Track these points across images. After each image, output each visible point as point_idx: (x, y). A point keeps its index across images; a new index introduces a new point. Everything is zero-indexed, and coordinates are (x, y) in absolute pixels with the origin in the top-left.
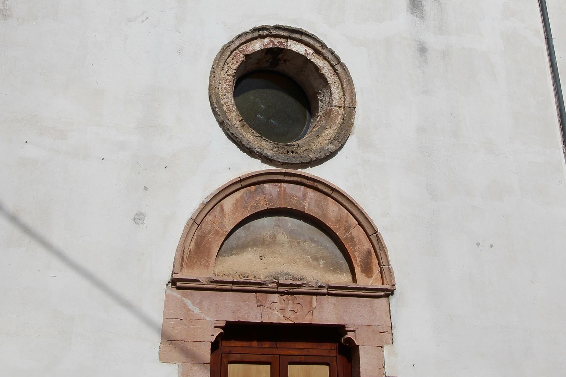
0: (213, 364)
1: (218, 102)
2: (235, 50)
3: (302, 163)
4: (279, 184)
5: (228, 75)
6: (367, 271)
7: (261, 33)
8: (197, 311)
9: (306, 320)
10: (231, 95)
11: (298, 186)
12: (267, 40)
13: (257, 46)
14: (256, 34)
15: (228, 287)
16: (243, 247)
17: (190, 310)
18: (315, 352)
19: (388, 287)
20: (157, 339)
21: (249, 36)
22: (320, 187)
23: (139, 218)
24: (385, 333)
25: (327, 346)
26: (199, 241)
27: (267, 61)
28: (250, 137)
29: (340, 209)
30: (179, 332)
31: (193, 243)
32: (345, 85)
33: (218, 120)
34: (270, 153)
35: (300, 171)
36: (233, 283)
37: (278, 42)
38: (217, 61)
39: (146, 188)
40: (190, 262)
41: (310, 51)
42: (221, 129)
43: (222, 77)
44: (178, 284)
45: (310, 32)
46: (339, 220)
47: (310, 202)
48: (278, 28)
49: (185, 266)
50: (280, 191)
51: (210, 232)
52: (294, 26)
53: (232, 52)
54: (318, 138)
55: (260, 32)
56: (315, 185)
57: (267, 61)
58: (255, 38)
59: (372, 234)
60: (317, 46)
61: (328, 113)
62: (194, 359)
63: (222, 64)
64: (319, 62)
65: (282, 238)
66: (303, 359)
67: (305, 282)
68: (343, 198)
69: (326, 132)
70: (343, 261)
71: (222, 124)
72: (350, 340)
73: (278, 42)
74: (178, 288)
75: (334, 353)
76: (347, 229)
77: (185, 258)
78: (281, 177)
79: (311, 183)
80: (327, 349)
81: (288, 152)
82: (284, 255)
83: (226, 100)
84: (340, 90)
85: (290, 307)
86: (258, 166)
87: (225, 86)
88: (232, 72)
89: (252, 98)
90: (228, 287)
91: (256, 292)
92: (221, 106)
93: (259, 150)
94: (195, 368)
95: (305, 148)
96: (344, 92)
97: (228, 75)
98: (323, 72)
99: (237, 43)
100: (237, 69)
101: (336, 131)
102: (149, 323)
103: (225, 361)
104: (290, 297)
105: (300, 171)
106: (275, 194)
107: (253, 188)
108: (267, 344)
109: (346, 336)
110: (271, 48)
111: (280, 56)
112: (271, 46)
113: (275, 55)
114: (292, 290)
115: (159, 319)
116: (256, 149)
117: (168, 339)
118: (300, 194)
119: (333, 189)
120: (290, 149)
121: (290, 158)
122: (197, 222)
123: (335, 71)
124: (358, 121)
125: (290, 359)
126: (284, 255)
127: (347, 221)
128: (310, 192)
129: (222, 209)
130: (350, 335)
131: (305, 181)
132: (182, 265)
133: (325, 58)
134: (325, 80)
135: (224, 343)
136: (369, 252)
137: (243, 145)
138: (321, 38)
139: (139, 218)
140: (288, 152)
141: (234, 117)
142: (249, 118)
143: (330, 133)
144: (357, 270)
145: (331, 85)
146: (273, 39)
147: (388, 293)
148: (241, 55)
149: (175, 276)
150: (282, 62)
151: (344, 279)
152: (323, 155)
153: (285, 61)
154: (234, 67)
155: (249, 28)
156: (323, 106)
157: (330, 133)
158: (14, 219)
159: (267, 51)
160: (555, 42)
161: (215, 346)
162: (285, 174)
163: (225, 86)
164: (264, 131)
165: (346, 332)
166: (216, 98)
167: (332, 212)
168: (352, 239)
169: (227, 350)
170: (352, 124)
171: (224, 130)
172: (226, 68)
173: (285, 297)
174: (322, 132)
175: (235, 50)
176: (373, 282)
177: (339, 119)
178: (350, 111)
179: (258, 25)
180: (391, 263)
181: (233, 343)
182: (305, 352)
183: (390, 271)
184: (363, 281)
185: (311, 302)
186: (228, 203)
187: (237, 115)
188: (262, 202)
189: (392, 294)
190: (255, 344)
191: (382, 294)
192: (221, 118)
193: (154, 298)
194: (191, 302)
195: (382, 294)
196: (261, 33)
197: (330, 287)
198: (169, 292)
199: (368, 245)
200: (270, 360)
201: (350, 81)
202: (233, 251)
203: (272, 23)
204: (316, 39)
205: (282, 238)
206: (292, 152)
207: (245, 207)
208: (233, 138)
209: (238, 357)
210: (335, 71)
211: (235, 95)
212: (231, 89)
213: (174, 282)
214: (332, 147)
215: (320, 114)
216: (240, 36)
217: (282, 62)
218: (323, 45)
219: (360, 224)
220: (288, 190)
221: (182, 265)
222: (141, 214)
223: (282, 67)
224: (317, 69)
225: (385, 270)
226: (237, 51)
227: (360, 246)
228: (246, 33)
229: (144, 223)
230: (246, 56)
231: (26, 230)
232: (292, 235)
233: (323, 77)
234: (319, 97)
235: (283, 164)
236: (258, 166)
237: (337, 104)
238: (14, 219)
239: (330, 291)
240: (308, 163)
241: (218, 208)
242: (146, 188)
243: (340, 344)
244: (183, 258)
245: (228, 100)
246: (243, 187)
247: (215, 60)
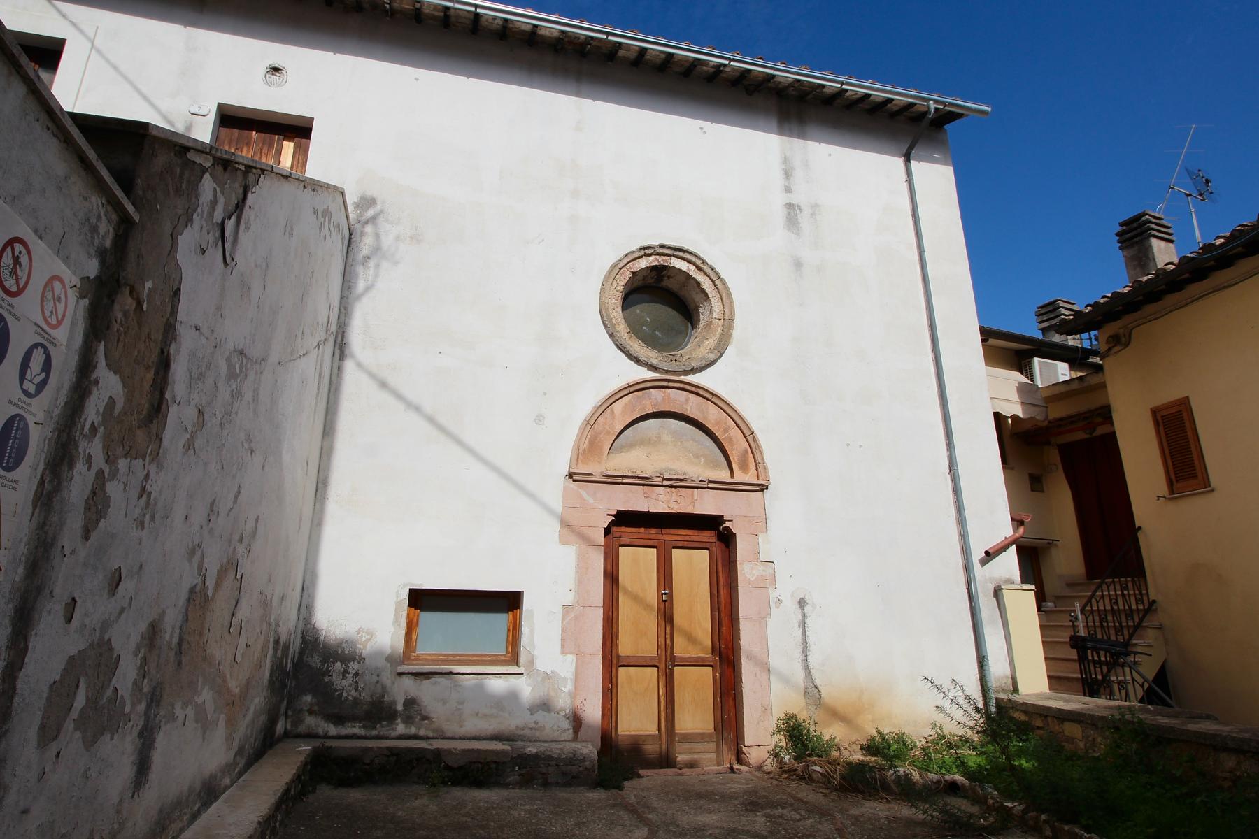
0: (606, 546)
1: (608, 316)
6: (744, 467)
8: (591, 501)
10: (619, 309)
12: (652, 258)
13: (644, 263)
14: (642, 253)
16: (631, 446)
18: (693, 538)
20: (557, 526)
21: (636, 255)
22: (701, 392)
23: (539, 419)
25: (707, 533)
28: (637, 347)
34: (655, 362)
35: (683, 378)
38: (607, 277)
39: (545, 393)
41: (693, 268)
45: (692, 250)
47: (692, 406)
48: (662, 246)
52: (677, 245)
54: (697, 347)
55: (646, 251)
56: (696, 390)
60: (699, 262)
64: (700, 277)
65: (666, 438)
66: (685, 544)
71: (611, 335)
72: (727, 528)
75: (714, 539)
76: (726, 430)
77: (580, 454)
80: (708, 536)
82: (670, 453)
85: (674, 498)
86: (645, 374)
88: (620, 288)
92: (610, 320)
94: (590, 549)
99: (625, 262)
102: (550, 511)
103: (616, 544)
105: (683, 378)
106: (660, 399)
108: (653, 531)
113: (659, 272)
114: (675, 484)
115: (558, 507)
116: (642, 358)
117: (567, 525)
119: (713, 395)
121: (673, 367)
122: (590, 423)
124: (737, 332)
126: (670, 453)
128: (692, 396)
130: (727, 524)
134: (706, 294)
135: (615, 529)
138: (702, 255)
139: (539, 419)
141: (622, 329)
142: (635, 330)
143: (710, 343)
147: (763, 488)
151: (724, 475)
152: (704, 363)
156: (703, 319)
157: (710, 343)
158: (431, 420)
159: (653, 269)
161: (607, 531)
162: (669, 381)
164: (650, 342)
167: (711, 415)
168: (730, 439)
176: (750, 478)
177: (719, 330)
178: (729, 322)
181: (623, 529)
182: (687, 538)
183: (765, 468)
184: (740, 477)
186: (618, 406)
190: (642, 530)
192: (611, 330)
193: (554, 489)
201: (729, 294)
202: (622, 449)
204: (697, 256)
205: (666, 438)
208: (622, 348)
209: (628, 541)
212: (619, 303)
213: (570, 475)
214: (712, 357)
218: (704, 262)
223: (666, 283)
224: (698, 284)
227: (737, 446)
231: (442, 429)
233: (703, 291)
235: (667, 372)
236: (645, 374)
238: (431, 420)
242: (545, 393)
245: (617, 314)
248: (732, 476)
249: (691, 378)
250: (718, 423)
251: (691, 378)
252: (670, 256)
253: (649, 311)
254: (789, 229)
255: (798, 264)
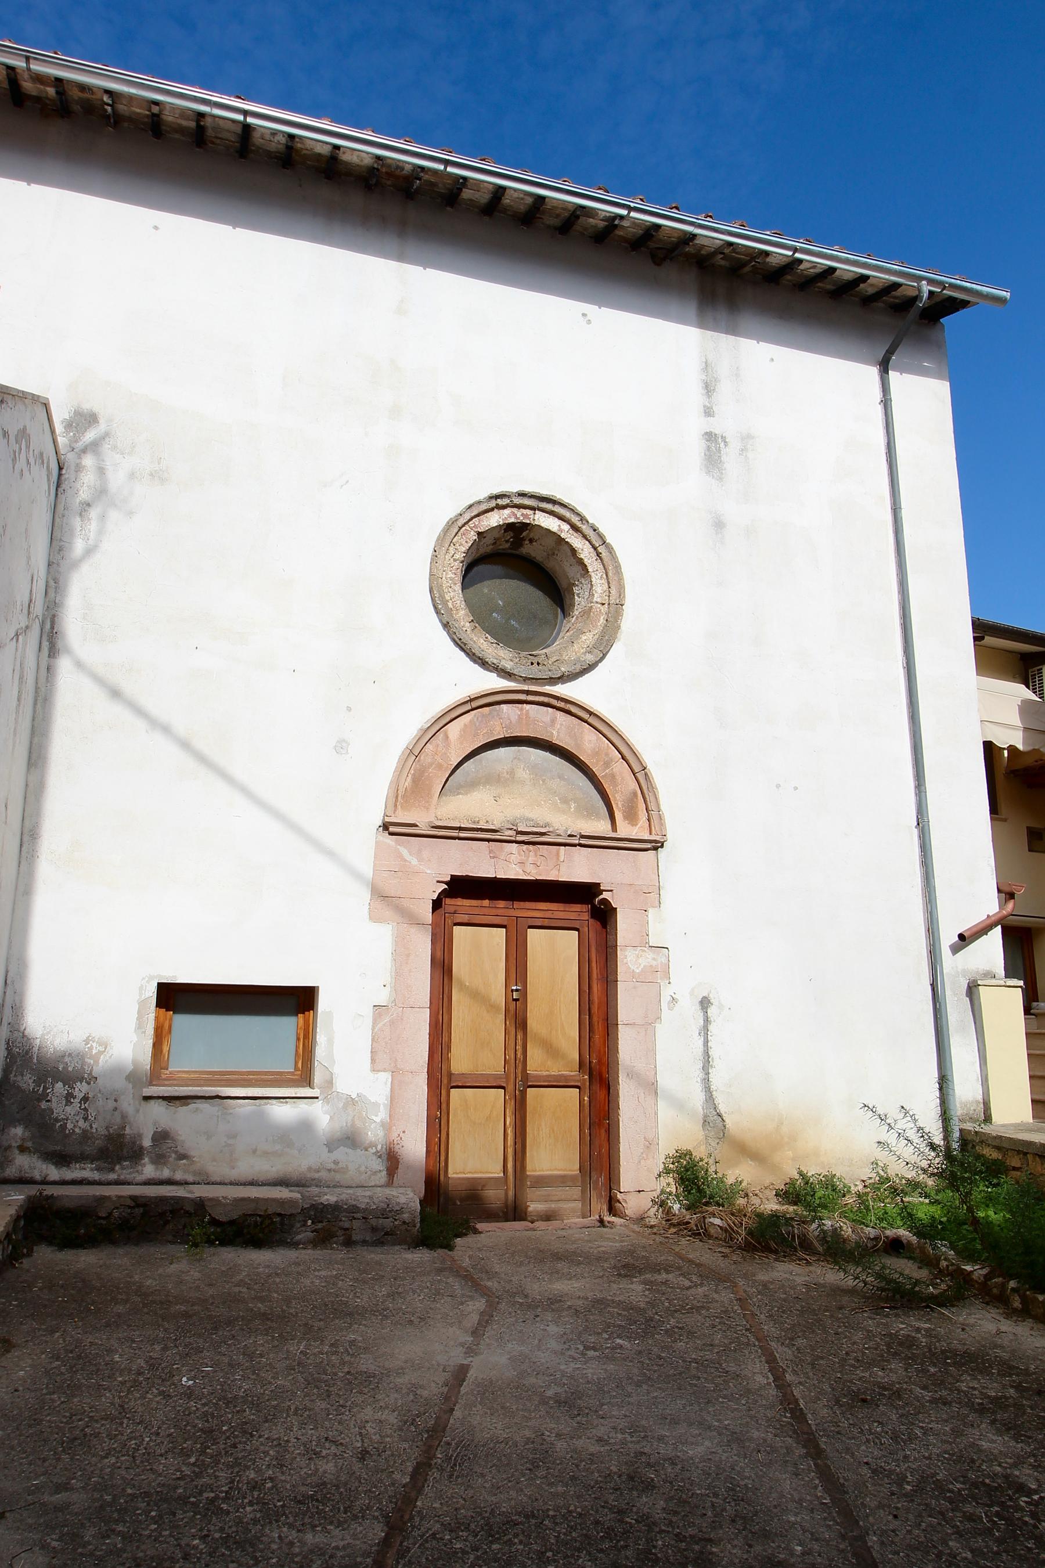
0: (434, 925)
1: (442, 597)
2: (463, 526)
3: (551, 678)
4: (520, 706)
5: (455, 560)
6: (631, 817)
7: (500, 502)
8: (414, 862)
9: (552, 876)
10: (458, 587)
11: (545, 708)
12: (507, 512)
13: (494, 520)
14: (493, 504)
15: (454, 834)
16: (472, 785)
17: (406, 861)
18: (561, 915)
19: (658, 838)
20: (366, 895)
21: (484, 507)
22: (573, 709)
23: (341, 746)
24: (651, 895)
25: (577, 907)
26: (416, 777)
27: (507, 541)
28: (483, 643)
29: (598, 739)
30: (392, 886)
31: (409, 779)
32: (610, 574)
33: (441, 621)
34: (508, 665)
35: (548, 689)
36: (460, 829)
37: (522, 515)
38: (440, 540)
39: (349, 709)
40: (406, 802)
41: (566, 527)
42: (445, 633)
43: (447, 562)
44: (392, 829)
45: (566, 500)
46: (597, 753)
47: (559, 728)
48: (522, 495)
49: (399, 807)
50: (522, 714)
51: (431, 764)
52: (545, 492)
53: (460, 528)
54: (570, 644)
55: (499, 501)
56: (567, 707)
57: (507, 541)
58: (492, 509)
59: (639, 772)
60: (575, 520)
61: (587, 612)
62: (412, 919)
63: (447, 546)
64: (576, 542)
65: (522, 774)
66: (546, 923)
67: (551, 829)
68: (603, 724)
69: (584, 638)
70: (601, 804)
71: (446, 626)
72: (605, 902)
73: (522, 515)
74: (391, 834)
75: (586, 916)
76: (607, 764)
77: (398, 797)
78: (523, 697)
79: (561, 705)
80: (578, 912)
81: (532, 664)
82: (524, 795)
83: (452, 594)
84: (604, 581)
85: (531, 859)
86: (494, 682)
87: (450, 575)
88: (460, 556)
89: (486, 591)
90: (454, 834)
91: (488, 840)
92: (445, 603)
93: (495, 661)
94: (413, 930)
95: (555, 658)
96: (609, 583)
97: (455, 560)
98: (582, 556)
99: (467, 516)
100: (467, 552)
101: (596, 637)
102: (357, 875)
103: (449, 922)
104: (531, 847)
105: (548, 689)
106: (514, 719)
107: (486, 710)
108: (501, 904)
109: (601, 897)
110: (513, 524)
111: (524, 534)
112: (512, 520)
113: (517, 531)
114: (533, 839)
115: (368, 871)
116: (490, 659)
117: (380, 895)
118: (547, 719)
119: (591, 713)
120: (535, 660)
121: (534, 672)
122: (414, 752)
123: (598, 554)
124: (627, 622)
125: (531, 922)
126: (524, 795)
127: (607, 754)
128: (559, 714)
129: (447, 737)
130: (605, 895)
131: (554, 702)
132: (396, 806)
133: (585, 537)
134: (584, 567)
135: (448, 901)
136: (635, 794)
137: (474, 654)
138: (580, 509)
139: (341, 746)
140: (532, 664)
141: (462, 617)
142: (481, 617)
143: (588, 638)
144: (618, 815)
145: (593, 574)
146: (515, 510)
147: (657, 846)
148: (472, 533)
149: (387, 819)
150: (527, 542)
151: (601, 827)
152: (578, 668)
153: (531, 541)
154: (464, 549)
155: (483, 495)
156: (580, 602)
157: (588, 638)
158: (185, 745)
159: (509, 527)
160: (905, 514)
161: (437, 904)
162: (528, 693)
163: (450, 575)
164: (502, 636)
165: (601, 892)
166: (439, 591)
167: (586, 743)
168: (613, 776)
169: (452, 909)
170: (619, 627)
171: (448, 633)
172: (452, 550)
173: (525, 847)
174: (578, 638)
175: (463, 526)
176: (639, 831)
177: (602, 620)
178: (616, 609)
179: (496, 491)
180: (662, 808)
181: (459, 902)
182: (548, 914)
183: (660, 818)
184: (625, 830)
185: (558, 854)
186: (454, 729)
187: (466, 615)
188: (498, 728)
189: (662, 846)
190: (486, 902)
191: (649, 846)
192: (445, 619)
193: (362, 844)
194: (407, 850)
195: (649, 846)
196: (500, 502)
197: (583, 837)
198: (381, 838)
199: (634, 785)
200: (505, 923)
201: (618, 568)
202: (458, 790)
203: (513, 488)
204: (573, 510)
205: (522, 774)
206: (538, 664)
207: (476, 735)
208: (461, 645)
209: (465, 918)
210: (598, 554)
211: (464, 587)
212: (459, 579)
213: (385, 826)
214: (590, 658)
215: (576, 613)
216: (470, 506)
217: (527, 542)
218: (583, 519)
219: (623, 758)
220: (532, 714)
221: (396, 806)
222: (344, 740)
223: (527, 549)
224: (574, 551)
225: (653, 815)
226: (467, 527)
227: (621, 788)
228: (479, 502)
229: (347, 753)
230: (480, 534)
231: (202, 759)
232: (536, 770)
233: (581, 563)
234: (576, 590)
235: (526, 680)
236: (494, 682)
237: (599, 600)
238: (185, 745)
239: (583, 841)
240: (559, 678)
241: (440, 735)
242: (349, 709)
243: (593, 906)
244: (397, 797)
245: (455, 594)
246: (473, 709)
247: (438, 540)
248: (614, 828)
249: (560, 690)
250: (596, 753)
251: (560, 690)
252: (533, 509)
253: (505, 590)
254: (708, 472)
255: (719, 525)
